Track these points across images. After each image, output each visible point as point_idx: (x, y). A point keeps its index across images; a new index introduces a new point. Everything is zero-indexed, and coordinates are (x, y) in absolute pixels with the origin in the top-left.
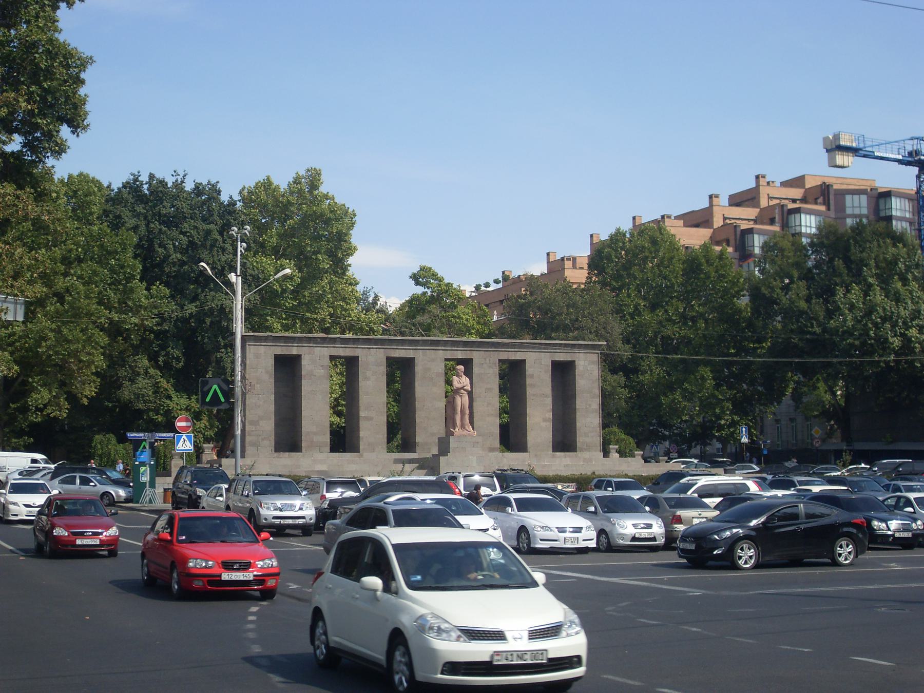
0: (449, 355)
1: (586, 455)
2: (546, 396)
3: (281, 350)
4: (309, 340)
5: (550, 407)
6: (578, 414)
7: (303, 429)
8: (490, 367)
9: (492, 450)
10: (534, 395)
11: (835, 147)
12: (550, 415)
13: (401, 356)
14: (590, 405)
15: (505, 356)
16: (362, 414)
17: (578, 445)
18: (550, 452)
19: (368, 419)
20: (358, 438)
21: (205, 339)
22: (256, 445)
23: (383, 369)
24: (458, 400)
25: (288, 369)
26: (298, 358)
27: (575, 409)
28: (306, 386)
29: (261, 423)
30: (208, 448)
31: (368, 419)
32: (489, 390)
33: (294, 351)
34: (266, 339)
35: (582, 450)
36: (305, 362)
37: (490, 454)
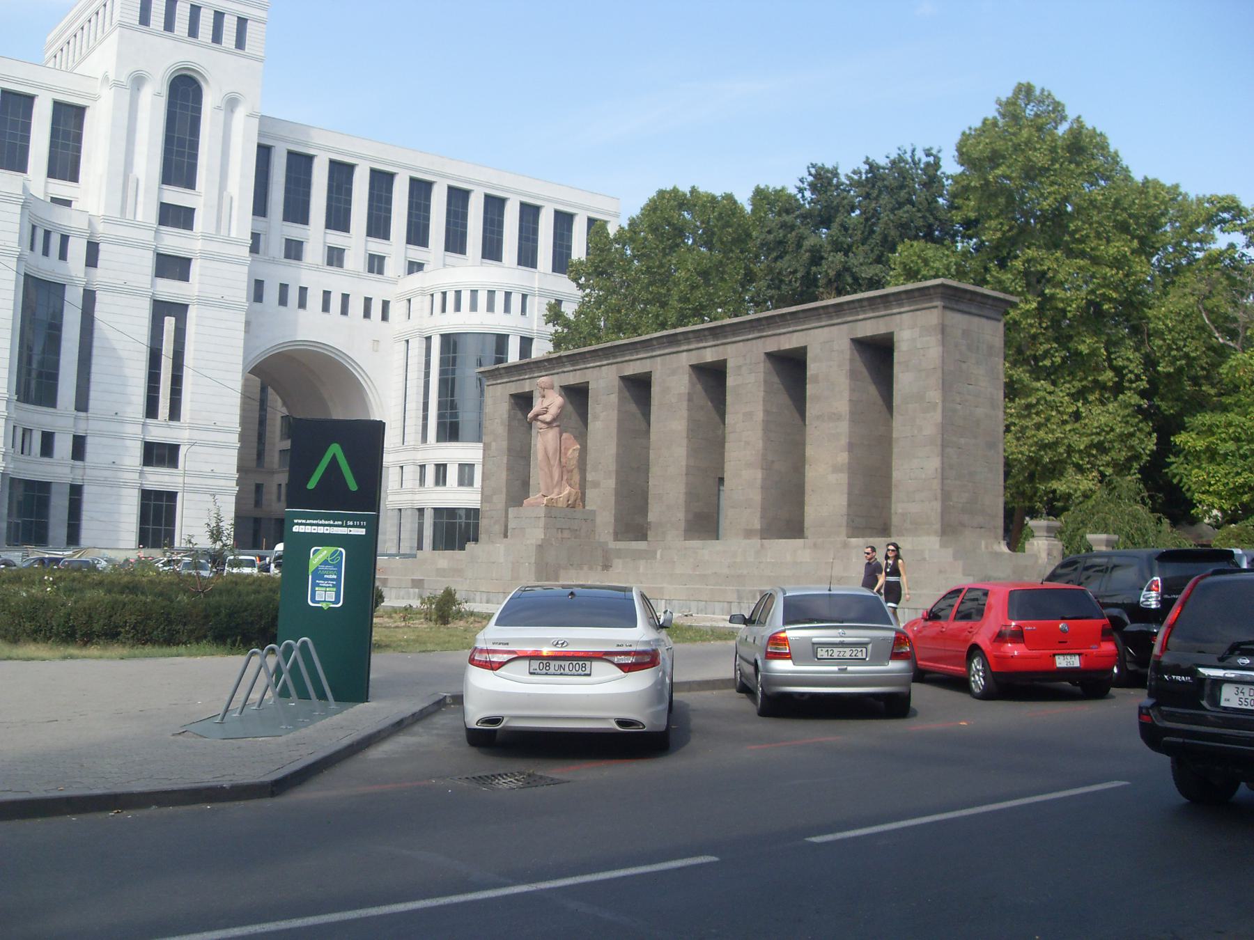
0: (695, 358)
3: (515, 388)
9: (749, 534)
10: (818, 417)
15: (773, 345)
17: (895, 520)
32: (749, 416)
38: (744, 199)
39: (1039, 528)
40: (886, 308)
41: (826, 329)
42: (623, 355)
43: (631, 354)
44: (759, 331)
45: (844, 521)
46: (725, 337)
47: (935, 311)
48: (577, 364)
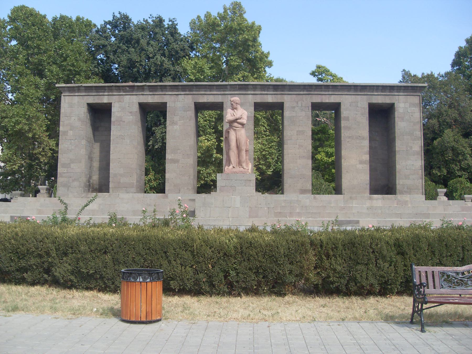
0: (259, 99)
1: (406, 197)
2: (364, 138)
4: (119, 89)
5: (367, 149)
6: (398, 156)
8: (302, 110)
9: (303, 191)
10: (349, 137)
12: (366, 157)
13: (209, 101)
14: (411, 148)
15: (317, 99)
17: (398, 187)
18: (367, 194)
19: (175, 161)
24: (233, 136)
25: (100, 115)
27: (395, 151)
28: (115, 131)
29: (72, 165)
30: (43, 189)
31: (175, 161)
32: (300, 133)
33: (105, 100)
34: (79, 89)
35: (402, 193)
36: (114, 110)
37: (302, 196)
38: (74, 19)
39: (441, 192)
40: (390, 92)
41: (353, 96)
43: (205, 91)
44: (307, 91)
46: (283, 91)
47: (418, 97)
48: (156, 91)
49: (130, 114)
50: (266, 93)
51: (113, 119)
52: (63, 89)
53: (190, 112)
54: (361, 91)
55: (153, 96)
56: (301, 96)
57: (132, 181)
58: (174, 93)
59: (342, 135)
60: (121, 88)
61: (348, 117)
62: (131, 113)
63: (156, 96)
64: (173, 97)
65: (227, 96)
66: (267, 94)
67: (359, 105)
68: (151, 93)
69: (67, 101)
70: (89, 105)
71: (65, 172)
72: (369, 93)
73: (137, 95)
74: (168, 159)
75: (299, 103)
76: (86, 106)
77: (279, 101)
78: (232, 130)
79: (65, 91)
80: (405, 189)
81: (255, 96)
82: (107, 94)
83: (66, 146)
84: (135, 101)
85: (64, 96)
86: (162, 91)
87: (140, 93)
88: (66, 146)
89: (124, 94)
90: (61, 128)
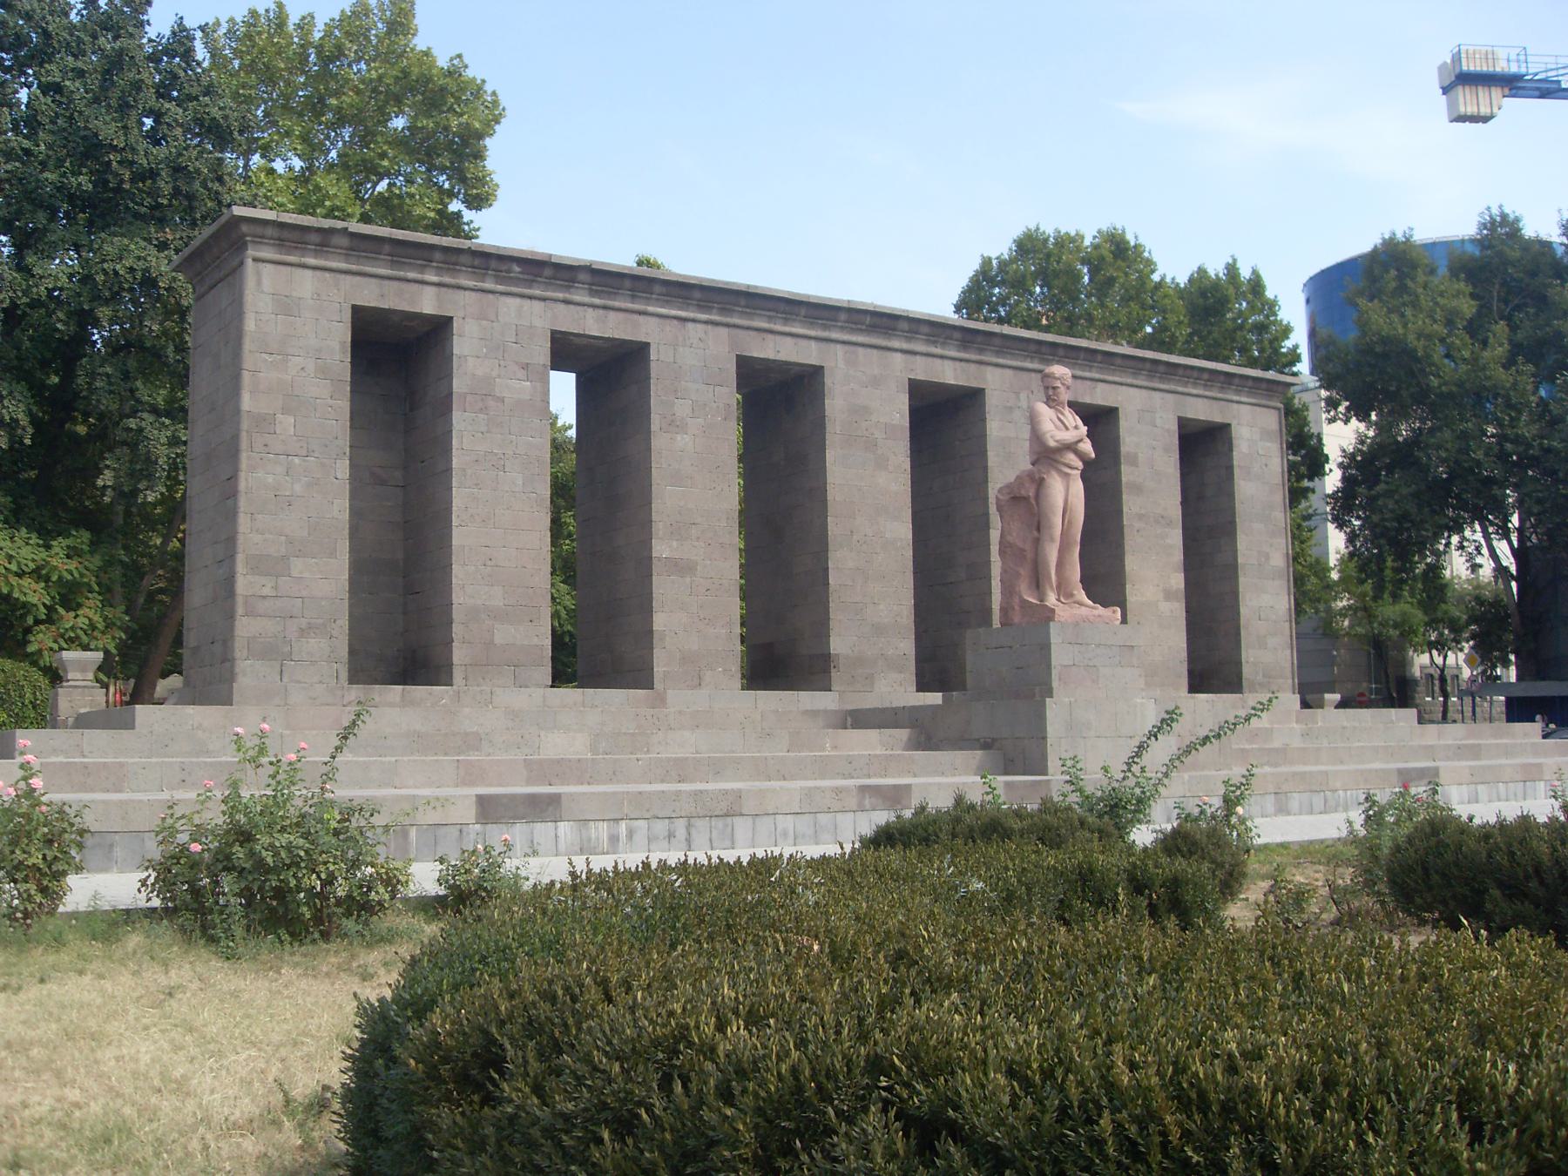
2: (1170, 524)
6: (1243, 581)
7: (457, 598)
10: (1141, 517)
11: (1474, 84)
12: (1178, 581)
14: (1267, 557)
16: (662, 549)
17: (1246, 671)
19: (682, 568)
20: (646, 636)
21: (98, 382)
22: (275, 653)
23: (729, 396)
26: (439, 328)
29: (297, 566)
30: (82, 666)
33: (427, 303)
35: (1253, 690)
36: (465, 345)
41: (1144, 392)
42: (750, 316)
43: (770, 319)
45: (1183, 670)
46: (981, 351)
48: (612, 295)
49: (521, 374)
50: (938, 351)
51: (459, 385)
52: (259, 230)
53: (724, 390)
54: (1162, 380)
55: (601, 312)
56: (1025, 375)
57: (536, 641)
58: (674, 312)
59: (1125, 509)
60: (493, 264)
61: (1136, 456)
62: (525, 367)
63: (612, 314)
64: (671, 328)
65: (832, 345)
66: (942, 357)
67: (1159, 422)
68: (597, 301)
69: (267, 284)
70: (356, 310)
71: (267, 591)
72: (1180, 389)
73: (544, 299)
74: (659, 559)
75: (1023, 396)
76: (347, 316)
77: (974, 384)
78: (1055, 474)
79: (260, 240)
80: (1260, 678)
81: (909, 357)
82: (435, 279)
83: (270, 479)
84: (538, 323)
85: (255, 260)
86: (633, 298)
87: (560, 295)
88: (270, 479)
89: (500, 288)
90: (247, 402)
